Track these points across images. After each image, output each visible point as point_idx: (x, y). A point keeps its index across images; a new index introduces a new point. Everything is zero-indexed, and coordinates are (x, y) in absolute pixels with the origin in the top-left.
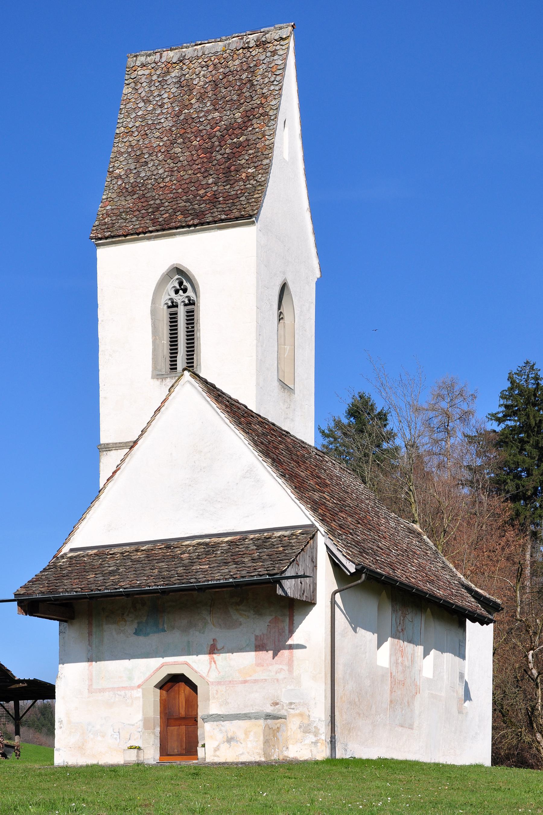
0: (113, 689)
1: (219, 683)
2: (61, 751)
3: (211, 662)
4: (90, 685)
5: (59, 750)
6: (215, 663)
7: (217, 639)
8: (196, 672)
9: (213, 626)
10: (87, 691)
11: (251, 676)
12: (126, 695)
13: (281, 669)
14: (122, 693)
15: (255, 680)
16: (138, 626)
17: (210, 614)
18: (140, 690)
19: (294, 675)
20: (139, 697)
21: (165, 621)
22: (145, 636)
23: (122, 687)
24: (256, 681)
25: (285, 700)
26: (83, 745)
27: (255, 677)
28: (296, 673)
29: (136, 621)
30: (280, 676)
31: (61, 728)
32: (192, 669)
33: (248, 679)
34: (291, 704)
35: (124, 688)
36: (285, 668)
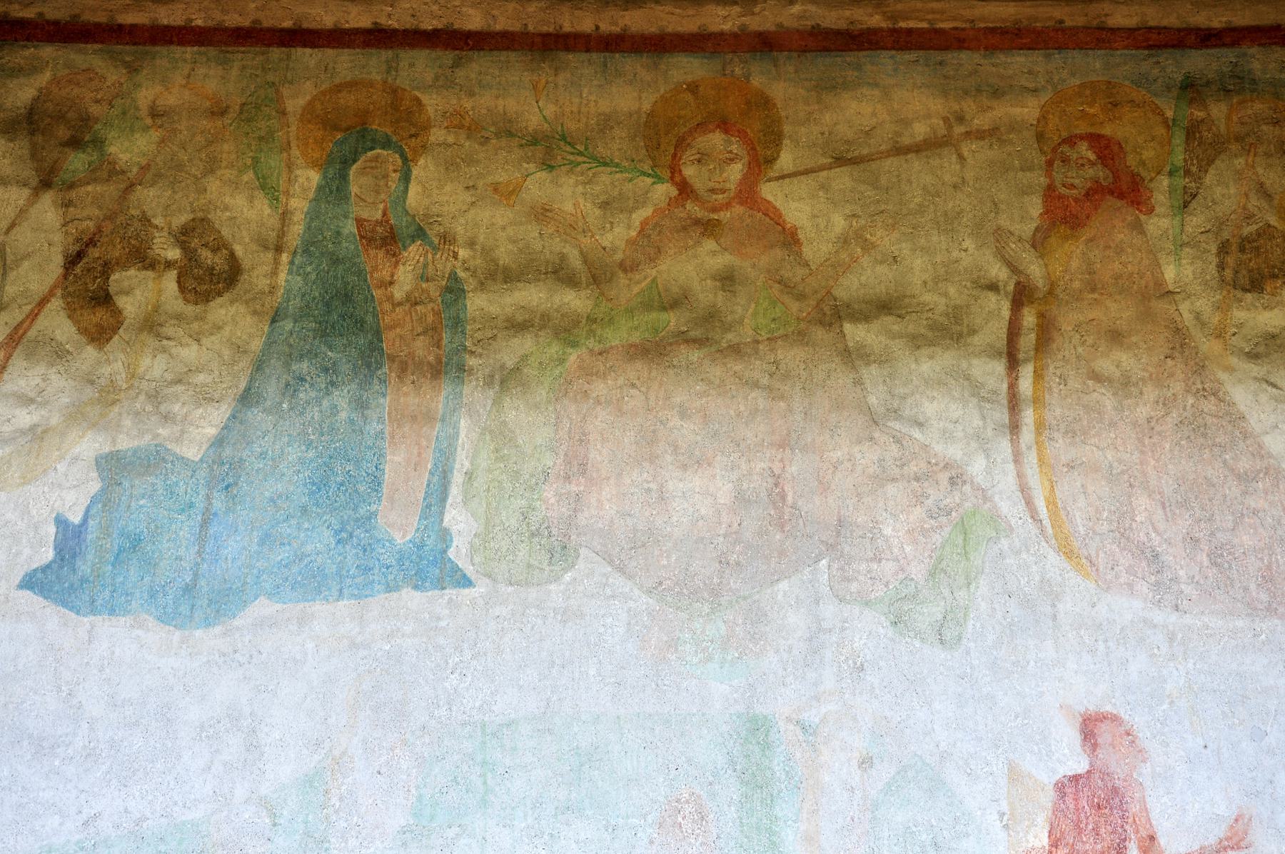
7: (1138, 720)
9: (1054, 560)
16: (104, 500)
17: (1014, 427)
21: (462, 461)
22: (168, 618)
29: (89, 445)
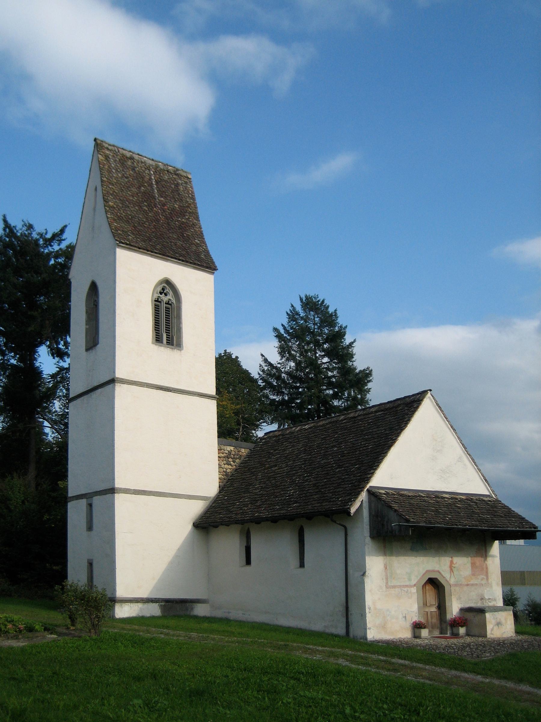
0: (400, 586)
1: (456, 585)
2: (371, 629)
3: (451, 571)
4: (387, 583)
5: (370, 629)
6: (453, 572)
8: (444, 577)
10: (385, 586)
11: (470, 581)
12: (408, 591)
13: (483, 578)
14: (406, 589)
15: (472, 584)
18: (415, 587)
19: (489, 581)
20: (415, 593)
23: (406, 585)
24: (472, 585)
25: (487, 598)
26: (385, 625)
27: (472, 582)
28: (490, 580)
30: (483, 582)
31: (370, 612)
32: (442, 575)
33: (469, 583)
34: (489, 599)
35: (407, 586)
36: (485, 577)
